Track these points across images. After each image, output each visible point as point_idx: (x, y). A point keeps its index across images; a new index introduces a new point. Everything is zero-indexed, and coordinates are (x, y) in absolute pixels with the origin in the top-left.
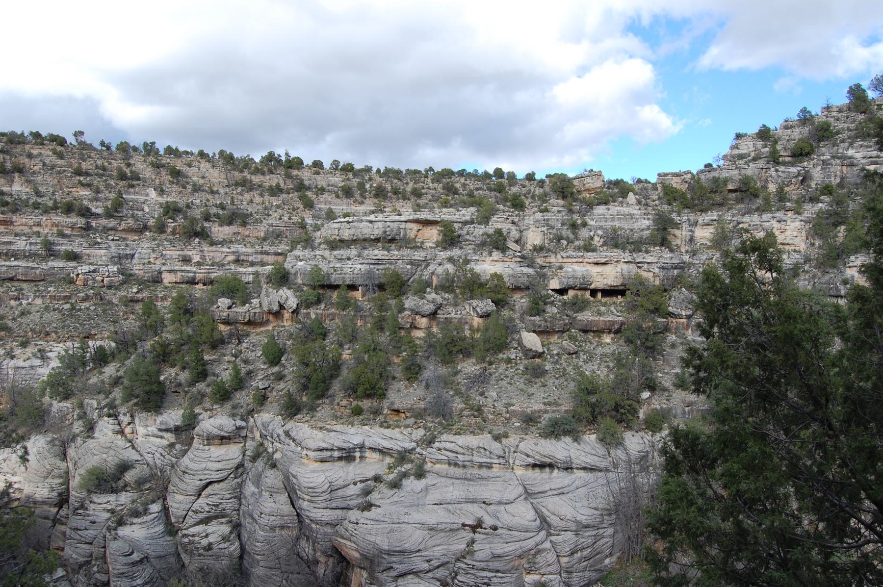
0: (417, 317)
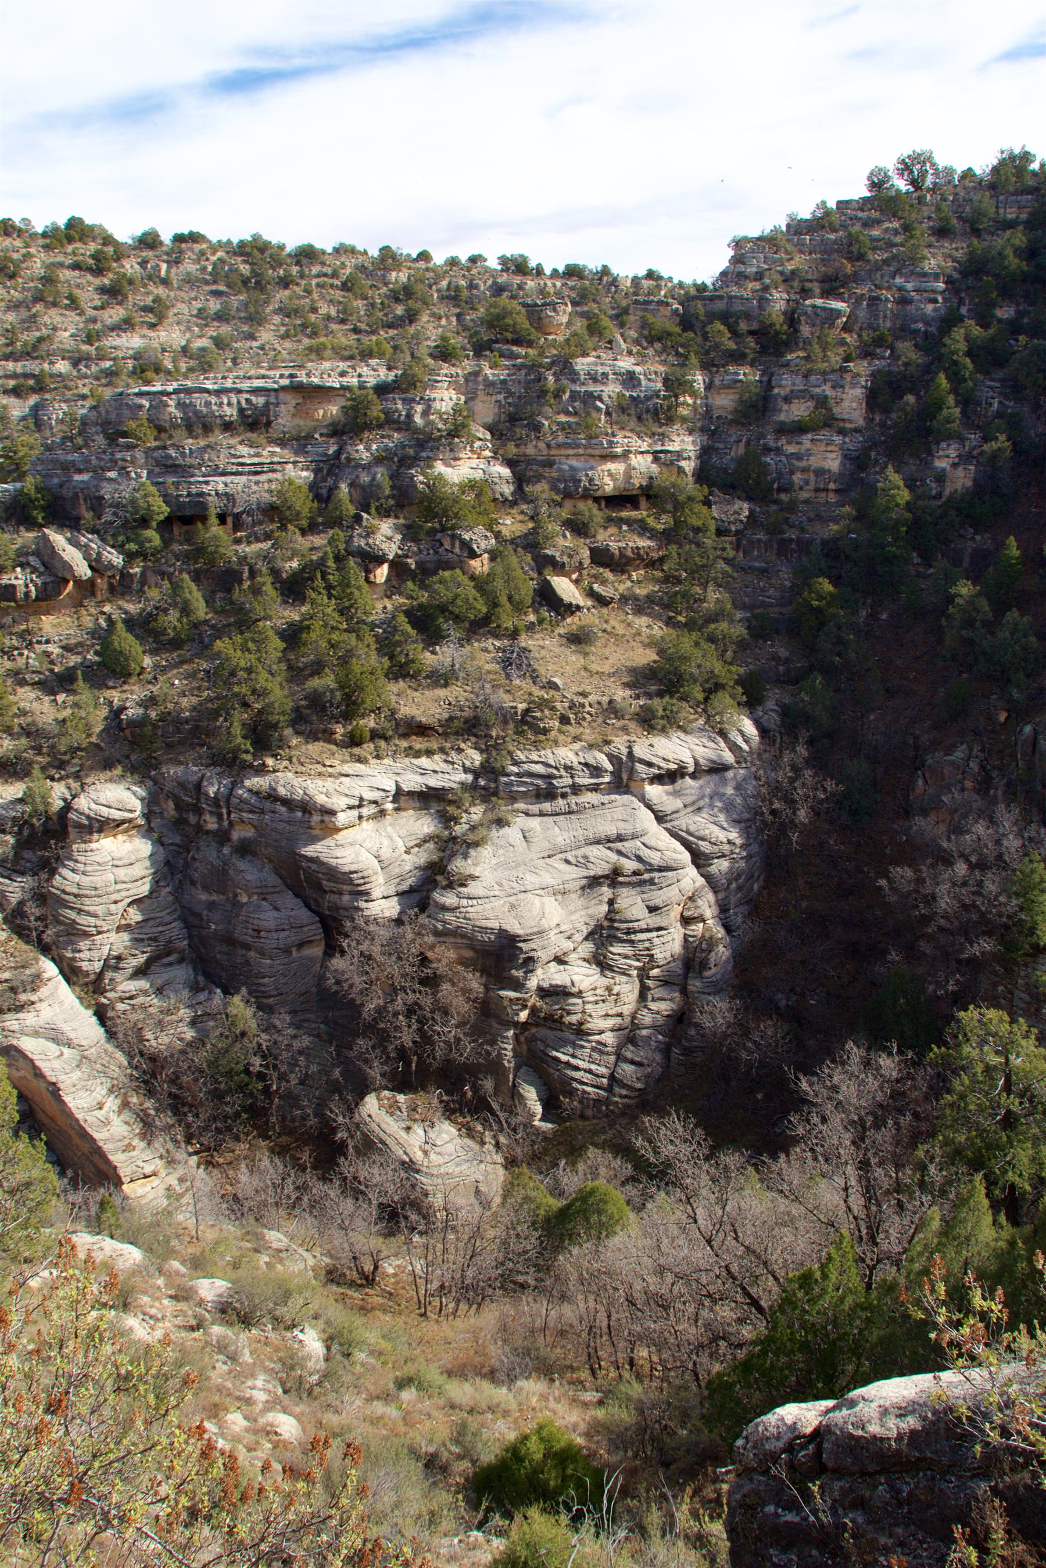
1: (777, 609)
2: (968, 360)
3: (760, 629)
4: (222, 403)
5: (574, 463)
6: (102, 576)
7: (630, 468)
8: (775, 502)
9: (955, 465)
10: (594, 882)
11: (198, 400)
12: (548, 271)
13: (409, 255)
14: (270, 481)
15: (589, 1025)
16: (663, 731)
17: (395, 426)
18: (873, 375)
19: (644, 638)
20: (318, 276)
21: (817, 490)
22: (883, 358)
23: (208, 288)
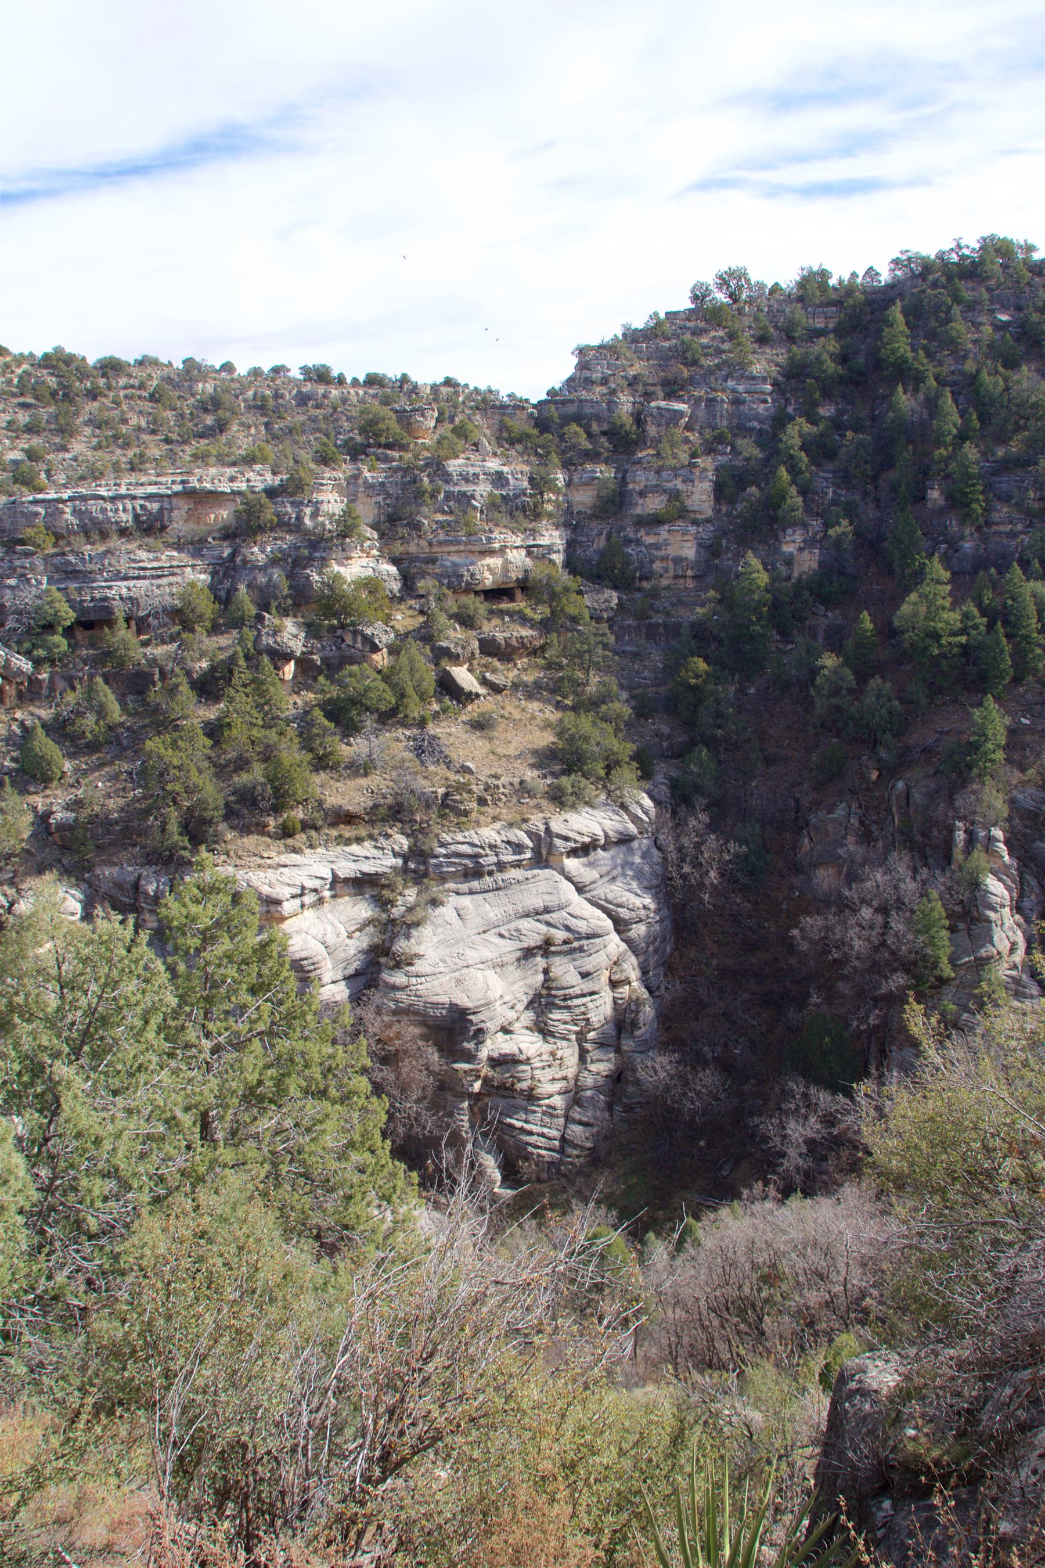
1: (653, 689)
2: (803, 454)
3: (643, 710)
4: (117, 510)
5: (455, 558)
6: (10, 682)
7: (507, 563)
8: (639, 590)
9: (801, 550)
10: (528, 953)
11: (93, 506)
12: (349, 381)
13: (212, 367)
14: (171, 584)
15: (539, 1090)
16: (573, 807)
18: (717, 469)
19: (539, 721)
20: (125, 388)
21: (676, 577)
22: (725, 454)
23: (15, 401)
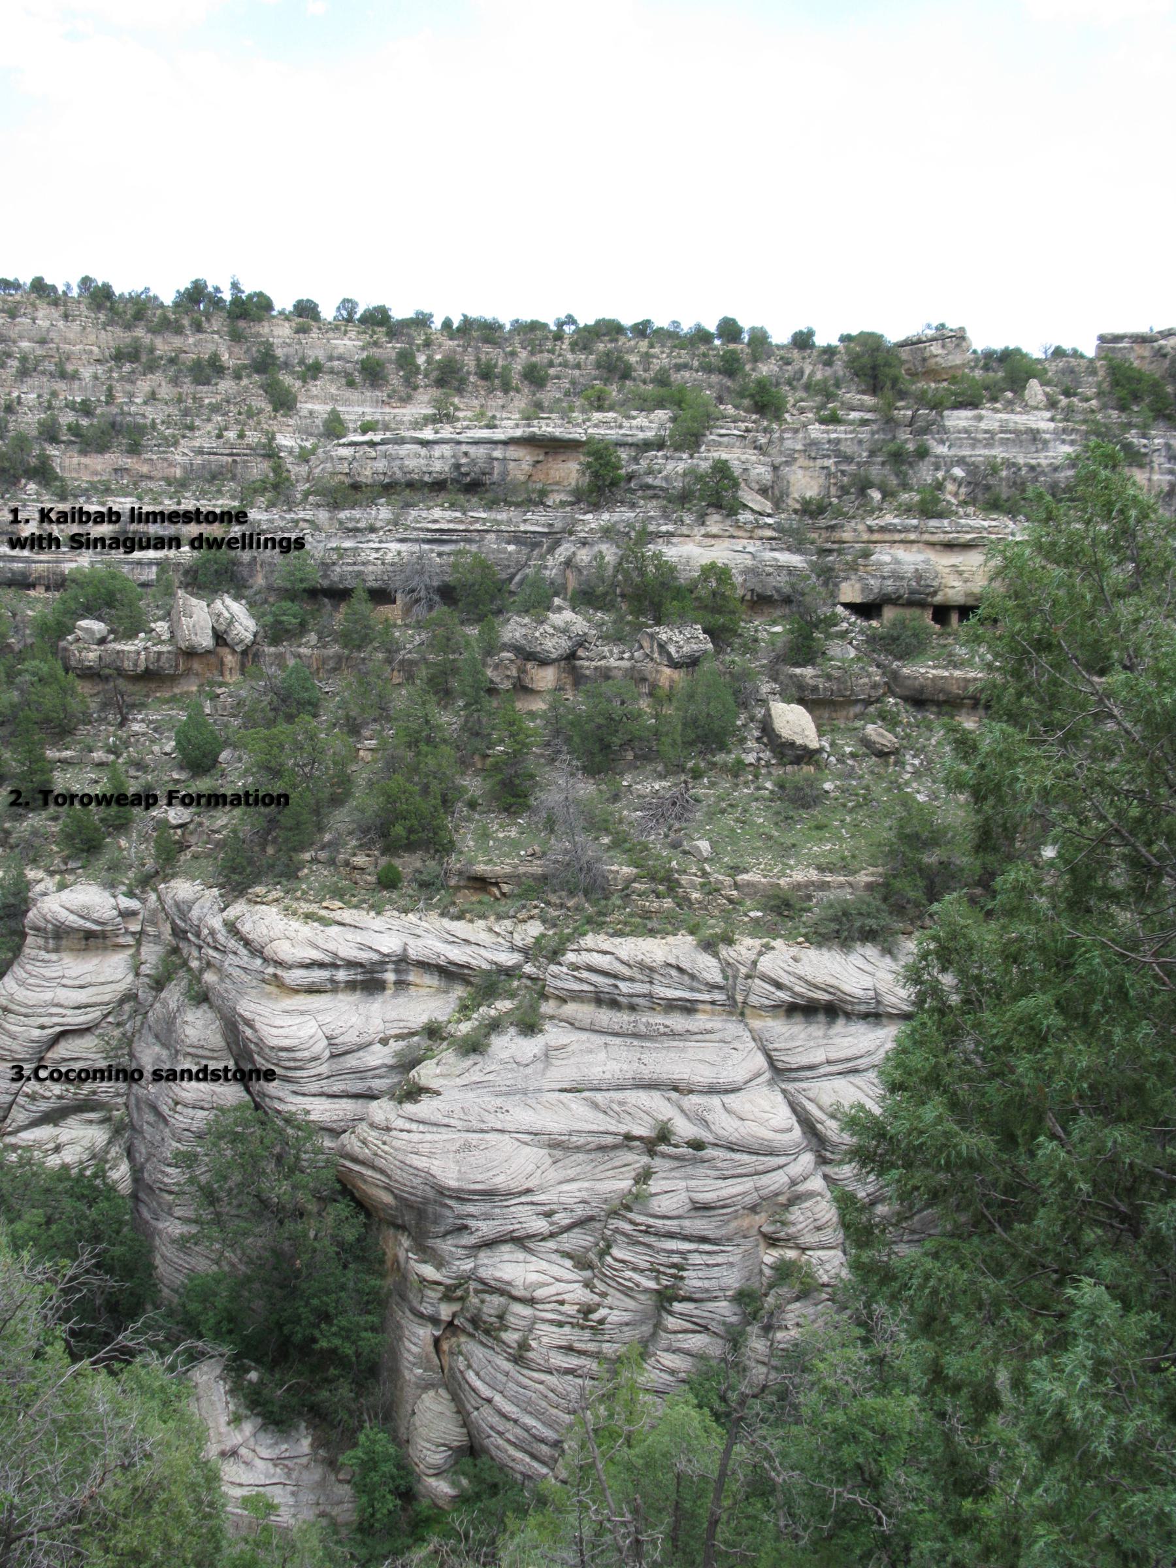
0: (529, 666)
17: (650, 492)
